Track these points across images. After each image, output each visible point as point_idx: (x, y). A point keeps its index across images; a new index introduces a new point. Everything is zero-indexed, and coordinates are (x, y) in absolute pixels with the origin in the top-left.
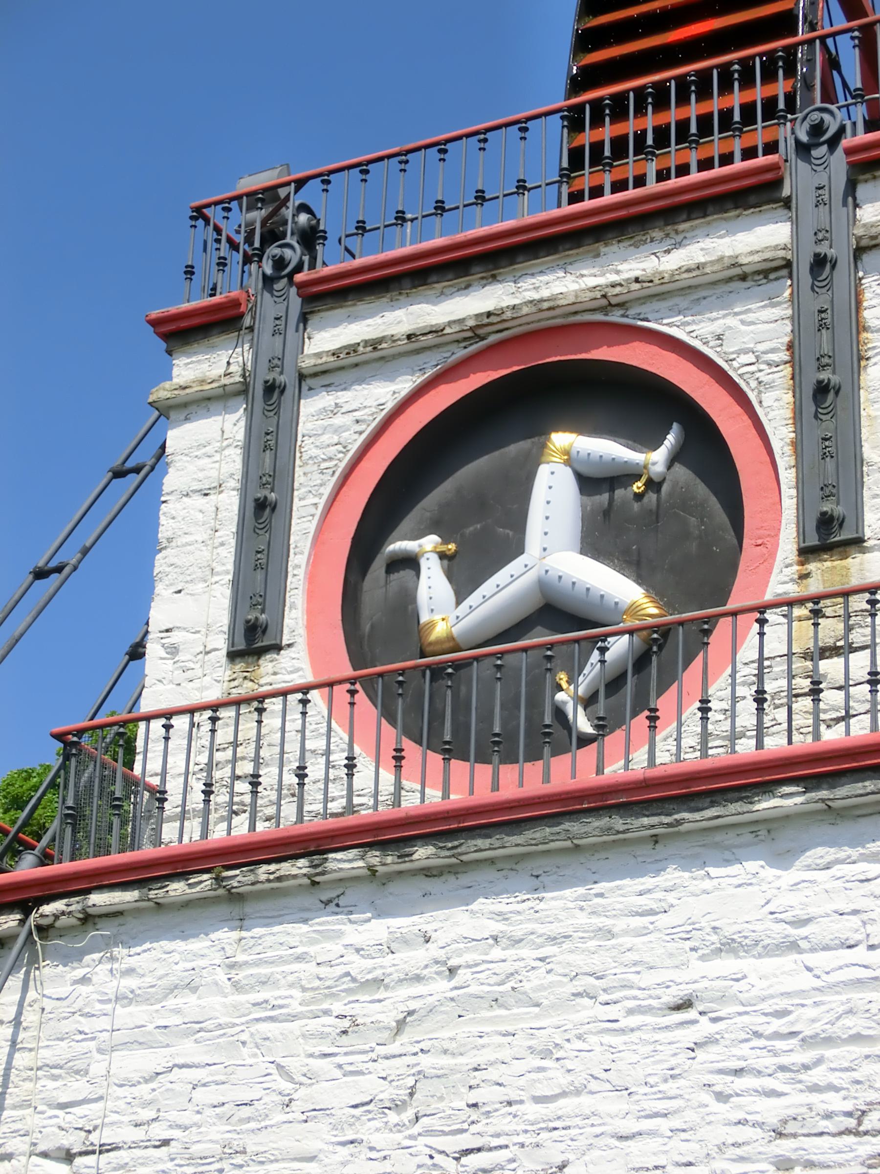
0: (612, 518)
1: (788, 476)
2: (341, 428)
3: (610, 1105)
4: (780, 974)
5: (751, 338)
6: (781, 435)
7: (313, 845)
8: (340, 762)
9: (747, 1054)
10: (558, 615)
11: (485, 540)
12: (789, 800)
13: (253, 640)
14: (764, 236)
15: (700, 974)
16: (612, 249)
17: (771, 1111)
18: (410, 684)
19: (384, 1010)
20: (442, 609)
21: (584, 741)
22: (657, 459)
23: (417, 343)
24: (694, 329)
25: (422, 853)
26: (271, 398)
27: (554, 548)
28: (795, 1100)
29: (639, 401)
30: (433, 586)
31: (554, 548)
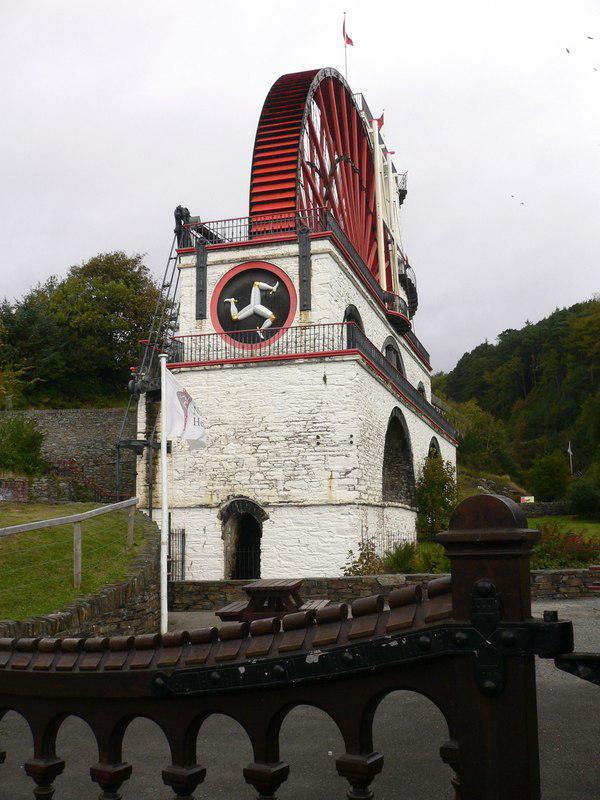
0: (266, 299)
1: (298, 296)
2: (216, 275)
3: (272, 408)
4: (297, 388)
5: (291, 268)
6: (297, 288)
7: (222, 363)
8: (222, 346)
9: (294, 401)
10: (258, 319)
11: (244, 301)
12: (301, 361)
13: (201, 316)
14: (294, 249)
15: (287, 387)
16: (267, 248)
17: (298, 409)
18: (227, 325)
19: (233, 391)
20: (236, 314)
21: (263, 340)
22: (274, 288)
23: (230, 262)
24: (280, 264)
25: (240, 365)
26: (201, 269)
27: (256, 305)
28: (301, 408)
29: (271, 275)
30: (233, 309)
31: (256, 305)
